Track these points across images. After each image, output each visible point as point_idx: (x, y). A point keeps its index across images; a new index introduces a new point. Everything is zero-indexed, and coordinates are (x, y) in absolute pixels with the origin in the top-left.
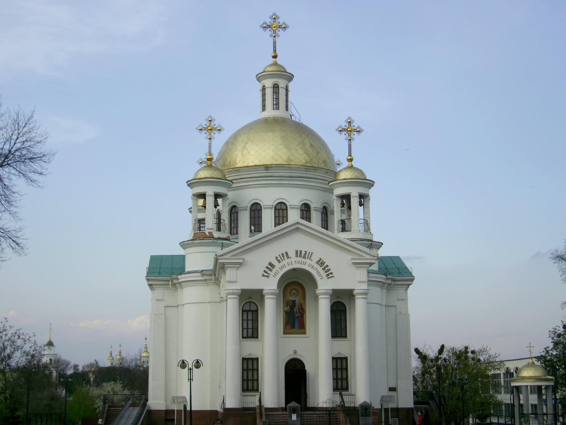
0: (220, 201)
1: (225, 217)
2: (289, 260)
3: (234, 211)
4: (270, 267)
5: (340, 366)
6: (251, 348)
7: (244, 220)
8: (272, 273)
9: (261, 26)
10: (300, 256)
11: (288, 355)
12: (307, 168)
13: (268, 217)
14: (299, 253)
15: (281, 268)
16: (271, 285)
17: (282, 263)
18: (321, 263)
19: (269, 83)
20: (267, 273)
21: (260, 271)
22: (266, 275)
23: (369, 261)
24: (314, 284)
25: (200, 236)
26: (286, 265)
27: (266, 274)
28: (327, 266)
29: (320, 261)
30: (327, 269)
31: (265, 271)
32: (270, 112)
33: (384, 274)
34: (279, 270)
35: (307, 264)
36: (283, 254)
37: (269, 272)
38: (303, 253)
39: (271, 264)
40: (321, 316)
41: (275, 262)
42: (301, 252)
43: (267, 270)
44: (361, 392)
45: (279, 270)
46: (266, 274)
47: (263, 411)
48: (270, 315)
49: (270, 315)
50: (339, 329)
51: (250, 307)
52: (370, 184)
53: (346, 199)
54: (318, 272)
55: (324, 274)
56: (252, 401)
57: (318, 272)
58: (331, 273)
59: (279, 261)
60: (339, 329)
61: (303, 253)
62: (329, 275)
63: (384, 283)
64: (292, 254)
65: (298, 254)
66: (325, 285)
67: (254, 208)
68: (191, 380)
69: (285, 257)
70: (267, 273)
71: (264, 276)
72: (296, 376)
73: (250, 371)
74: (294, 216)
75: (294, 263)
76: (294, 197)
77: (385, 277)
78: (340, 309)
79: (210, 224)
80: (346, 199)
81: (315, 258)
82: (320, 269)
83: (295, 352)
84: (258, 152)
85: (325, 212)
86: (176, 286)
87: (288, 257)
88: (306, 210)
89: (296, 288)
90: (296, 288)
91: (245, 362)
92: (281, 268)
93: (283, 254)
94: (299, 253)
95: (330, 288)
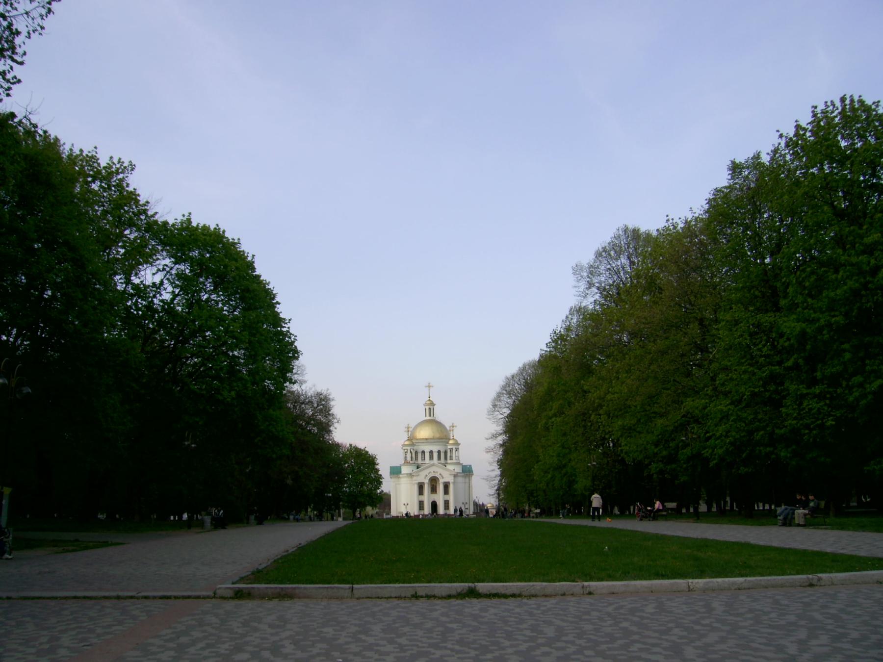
3: (416, 453)
5: (447, 503)
6: (422, 498)
7: (420, 456)
12: (439, 438)
16: (426, 481)
19: (427, 408)
21: (424, 477)
25: (406, 462)
32: (428, 418)
40: (441, 488)
44: (451, 511)
48: (426, 489)
49: (426, 489)
50: (446, 491)
51: (421, 487)
52: (459, 444)
53: (451, 450)
56: (422, 512)
60: (446, 491)
66: (441, 481)
72: (434, 506)
73: (421, 505)
75: (433, 475)
76: (435, 448)
78: (446, 486)
79: (409, 459)
80: (451, 450)
84: (424, 433)
85: (446, 452)
86: (399, 478)
88: (439, 452)
89: (434, 481)
90: (434, 481)
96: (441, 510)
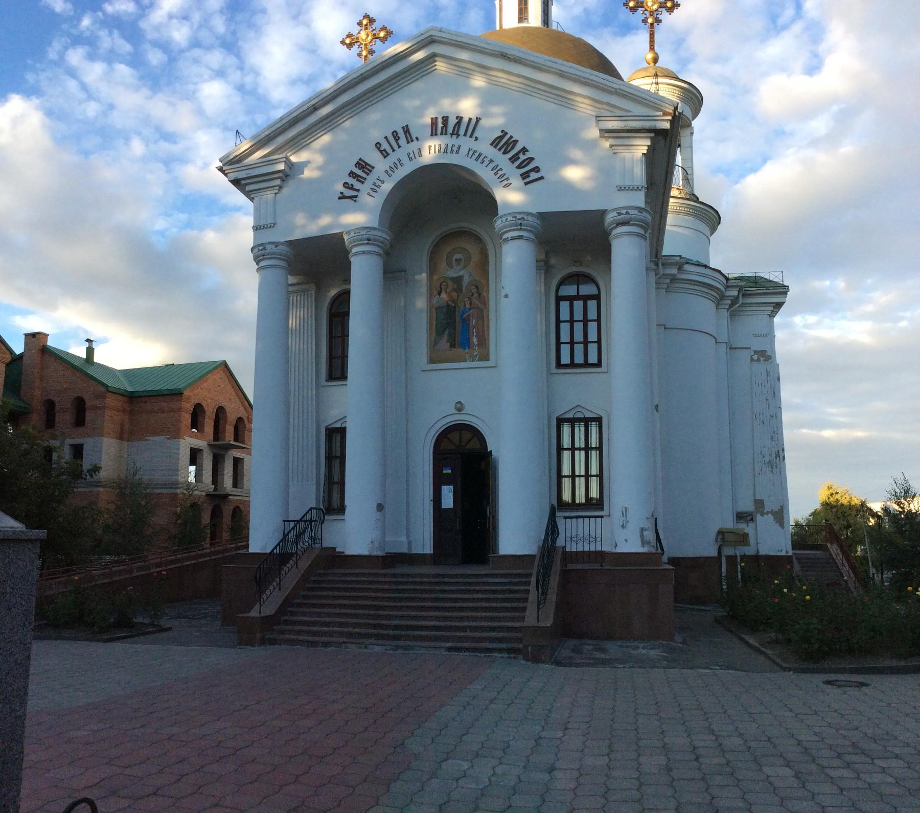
4: (359, 172)
8: (364, 188)
11: (434, 416)
17: (393, 158)
18: (504, 143)
22: (349, 196)
26: (405, 160)
27: (348, 193)
29: (500, 138)
34: (384, 177)
37: (357, 185)
39: (362, 165)
41: (373, 158)
45: (384, 177)
54: (496, 169)
57: (496, 169)
58: (536, 169)
59: (385, 154)
82: (503, 160)
93: (395, 134)
95: (534, 211)
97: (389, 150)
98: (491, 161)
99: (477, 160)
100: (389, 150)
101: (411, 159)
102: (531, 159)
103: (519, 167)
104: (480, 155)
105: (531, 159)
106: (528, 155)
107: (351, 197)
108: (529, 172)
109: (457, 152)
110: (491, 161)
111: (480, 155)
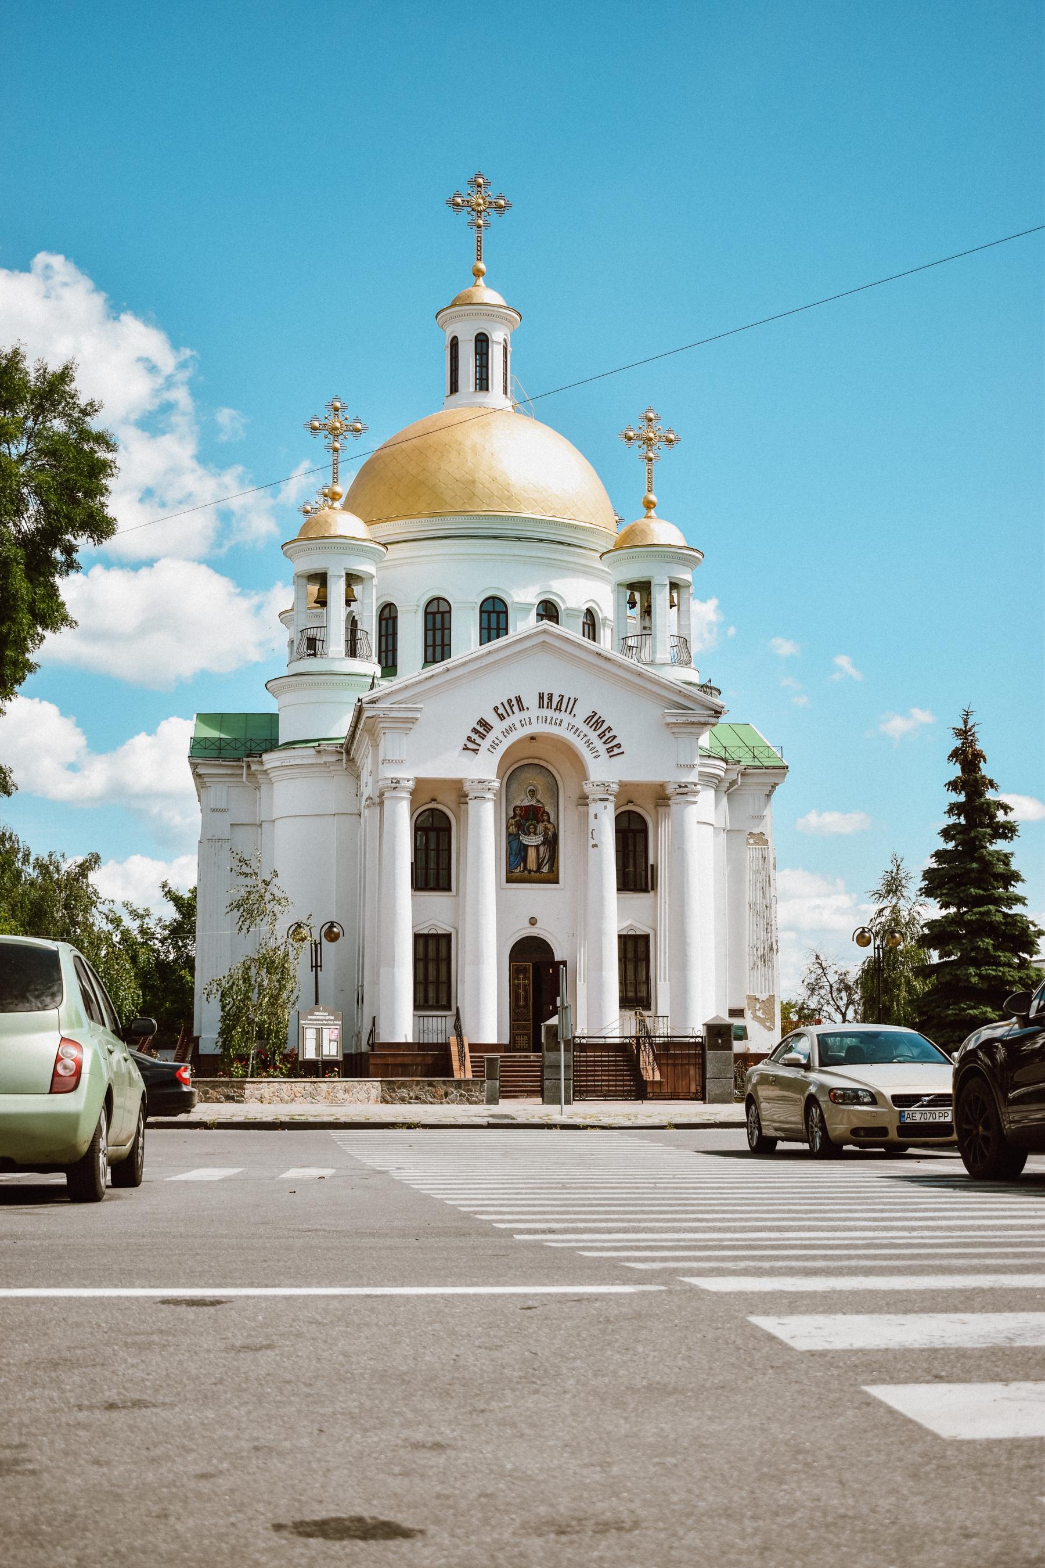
0: (357, 589)
1: (369, 625)
2: (525, 715)
3: (388, 616)
4: (481, 730)
8: (485, 744)
9: (447, 202)
10: (549, 706)
13: (465, 629)
14: (546, 700)
15: (507, 732)
16: (483, 769)
17: (508, 722)
18: (595, 721)
20: (474, 742)
22: (471, 747)
23: (702, 720)
24: (581, 771)
26: (518, 725)
28: (609, 729)
30: (608, 735)
31: (469, 739)
33: (722, 759)
34: (501, 737)
35: (565, 724)
36: (509, 701)
37: (478, 740)
38: (556, 700)
39: (483, 723)
41: (492, 719)
42: (551, 696)
43: (474, 736)
46: (471, 745)
47: (467, 1049)
54: (589, 743)
55: (602, 748)
57: (589, 743)
58: (619, 746)
59: (502, 717)
61: (556, 700)
62: (614, 749)
63: (721, 780)
64: (531, 701)
65: (544, 700)
66: (603, 771)
67: (433, 608)
68: (316, 966)
69: (516, 708)
70: (474, 742)
71: (466, 748)
72: (537, 975)
74: (524, 624)
75: (534, 722)
77: (723, 764)
81: (582, 711)
82: (593, 736)
83: (533, 921)
87: (521, 708)
91: (421, 942)
92: (507, 732)
93: (509, 701)
94: (546, 700)
96: (597, 1011)
97: (505, 715)
98: (585, 735)
99: (575, 733)
100: (505, 715)
101: (523, 726)
102: (615, 737)
103: (604, 743)
104: (577, 730)
105: (615, 737)
106: (612, 733)
107: (474, 750)
108: (614, 749)
109: (560, 725)
110: (585, 735)
111: (577, 730)
